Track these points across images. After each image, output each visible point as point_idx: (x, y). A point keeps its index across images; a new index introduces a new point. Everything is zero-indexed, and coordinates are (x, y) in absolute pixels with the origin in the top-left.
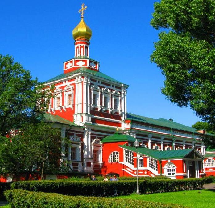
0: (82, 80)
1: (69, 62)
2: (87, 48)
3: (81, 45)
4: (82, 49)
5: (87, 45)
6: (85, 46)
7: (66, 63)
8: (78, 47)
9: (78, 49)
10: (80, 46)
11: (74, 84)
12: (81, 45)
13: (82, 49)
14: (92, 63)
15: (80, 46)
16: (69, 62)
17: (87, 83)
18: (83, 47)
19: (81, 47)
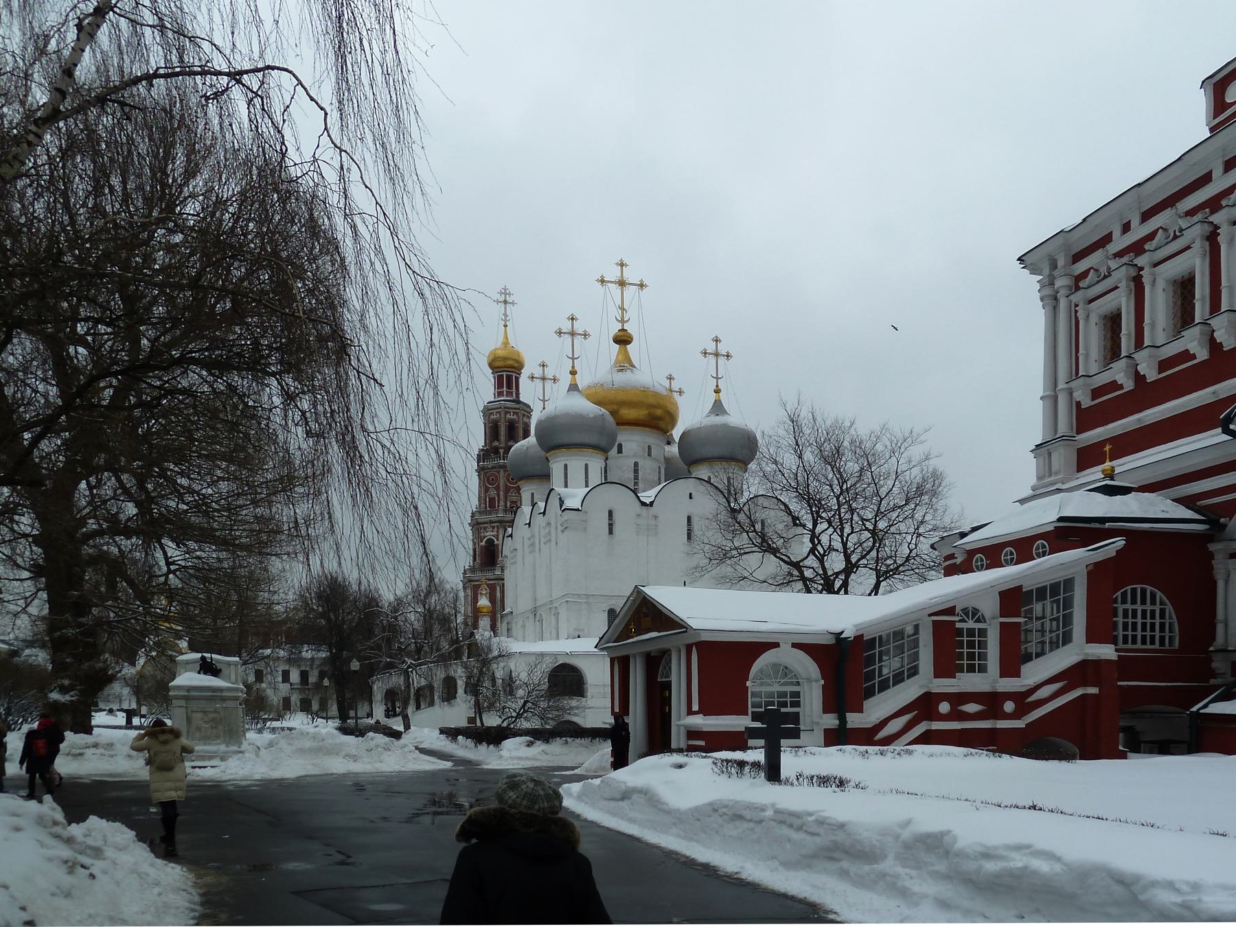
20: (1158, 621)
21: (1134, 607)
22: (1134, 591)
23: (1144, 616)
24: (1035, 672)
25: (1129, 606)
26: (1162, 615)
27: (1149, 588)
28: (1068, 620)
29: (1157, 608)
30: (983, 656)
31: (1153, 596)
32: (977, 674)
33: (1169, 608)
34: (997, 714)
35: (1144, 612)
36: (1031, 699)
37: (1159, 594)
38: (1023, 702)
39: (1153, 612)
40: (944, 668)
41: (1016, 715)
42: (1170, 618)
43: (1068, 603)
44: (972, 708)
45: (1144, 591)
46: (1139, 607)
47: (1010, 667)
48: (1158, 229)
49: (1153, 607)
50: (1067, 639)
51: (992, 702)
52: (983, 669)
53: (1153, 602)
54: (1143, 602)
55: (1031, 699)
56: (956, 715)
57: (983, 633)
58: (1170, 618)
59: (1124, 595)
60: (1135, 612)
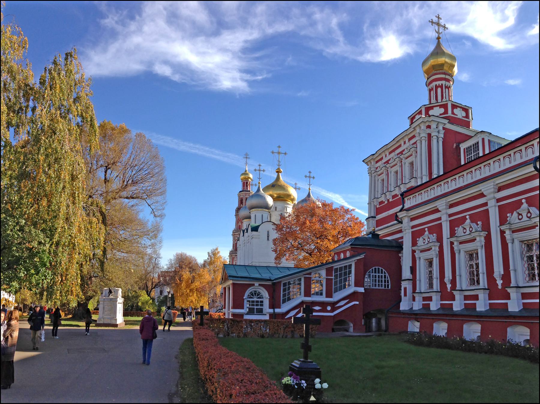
0: (428, 131)
1: (416, 115)
2: (448, 88)
3: (438, 85)
4: (439, 90)
5: (447, 83)
6: (445, 85)
7: (412, 118)
8: (432, 89)
9: (432, 92)
10: (436, 85)
11: (415, 143)
12: (438, 85)
13: (439, 90)
14: (459, 109)
15: (436, 85)
16: (416, 115)
17: (438, 138)
18: (441, 87)
19: (437, 87)
20: (383, 279)
21: (375, 274)
22: (375, 269)
23: (379, 278)
25: (374, 274)
26: (385, 277)
27: (380, 268)
29: (383, 275)
31: (382, 270)
33: (387, 274)
35: (379, 276)
37: (384, 270)
39: (382, 276)
42: (387, 278)
43: (350, 272)
45: (379, 269)
46: (377, 274)
49: (382, 274)
53: (382, 273)
54: (379, 273)
58: (387, 278)
59: (372, 270)
60: (376, 276)
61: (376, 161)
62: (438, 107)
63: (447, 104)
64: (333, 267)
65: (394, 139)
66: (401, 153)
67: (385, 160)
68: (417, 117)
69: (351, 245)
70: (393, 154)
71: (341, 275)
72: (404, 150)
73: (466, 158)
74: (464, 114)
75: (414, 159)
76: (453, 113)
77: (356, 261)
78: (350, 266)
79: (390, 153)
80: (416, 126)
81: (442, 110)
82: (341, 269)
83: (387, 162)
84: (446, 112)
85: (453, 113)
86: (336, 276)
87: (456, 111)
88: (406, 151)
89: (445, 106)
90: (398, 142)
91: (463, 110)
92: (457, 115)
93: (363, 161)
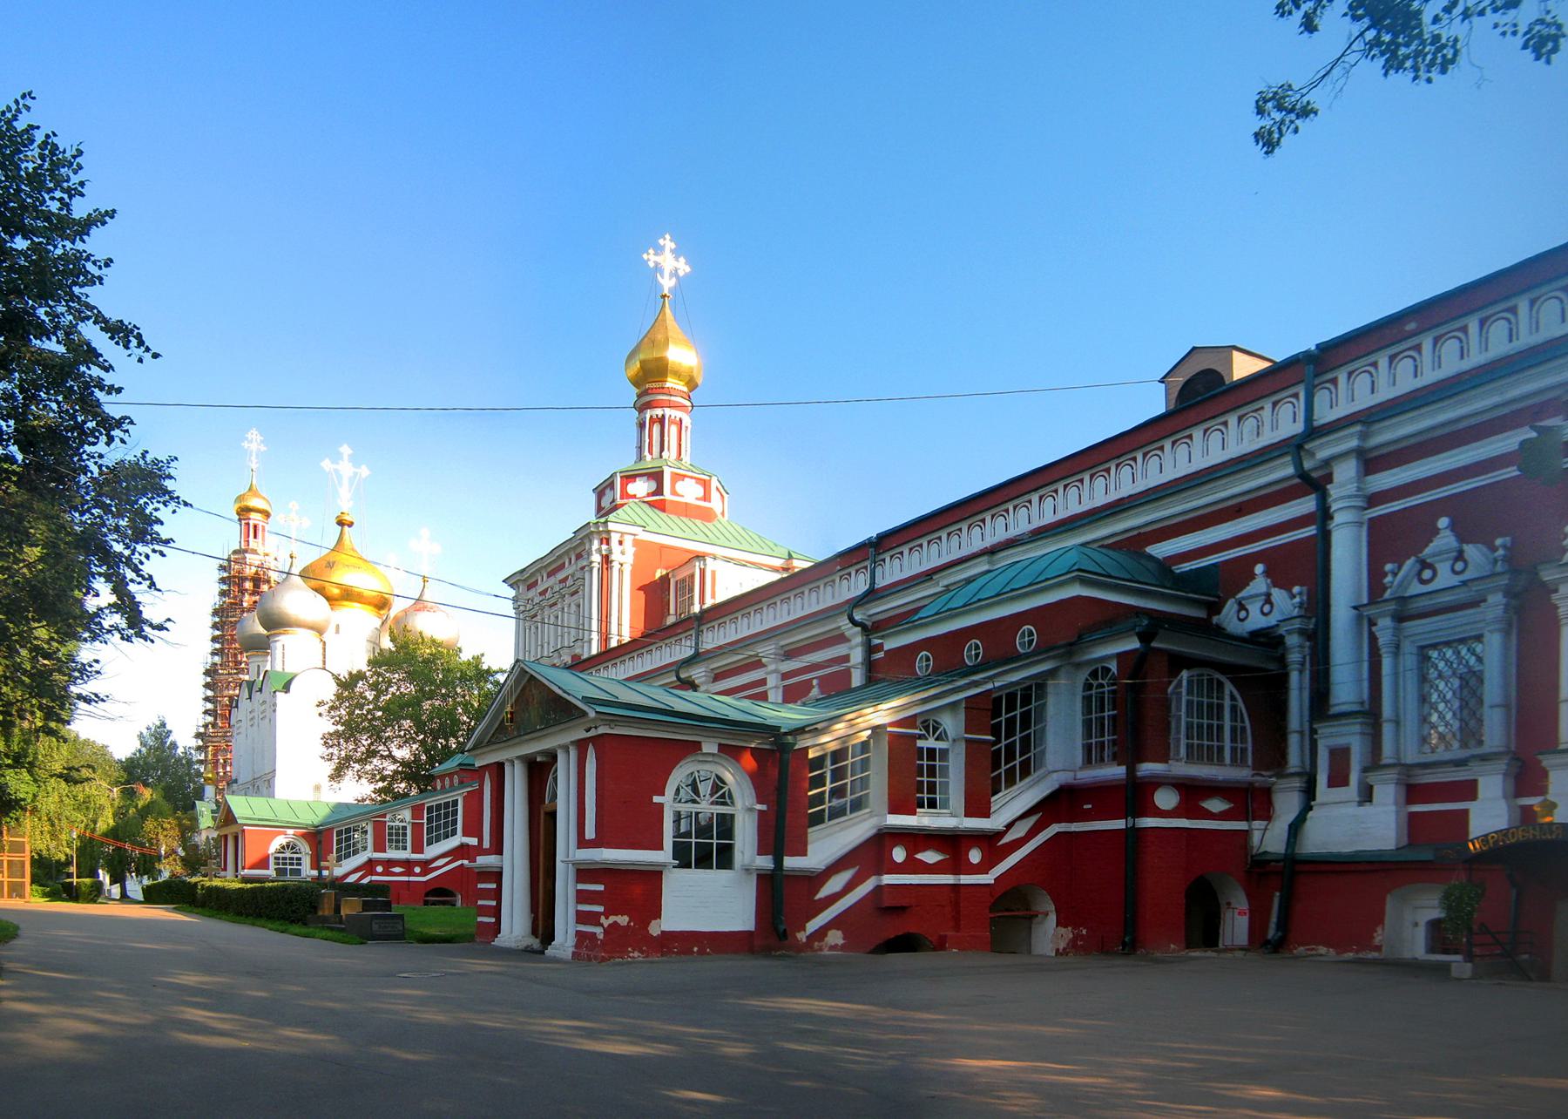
11: (583, 568)
16: (605, 488)
24: (431, 851)
28: (455, 822)
30: (404, 841)
32: (401, 851)
34: (409, 872)
36: (434, 865)
38: (426, 866)
40: (379, 847)
41: (423, 874)
43: (455, 813)
44: (398, 870)
47: (418, 848)
48: (547, 589)
50: (454, 833)
51: (408, 865)
52: (405, 848)
55: (434, 865)
56: (386, 873)
57: (404, 828)
61: (529, 583)
62: (645, 478)
63: (663, 472)
64: (424, 804)
65: (551, 552)
66: (565, 579)
67: (540, 588)
68: (608, 491)
69: (460, 764)
70: (552, 580)
71: (438, 817)
72: (566, 578)
73: (679, 600)
74: (700, 491)
75: (581, 600)
76: (674, 493)
77: (465, 794)
78: (455, 803)
79: (549, 575)
80: (585, 536)
81: (653, 486)
82: (439, 807)
83: (543, 593)
84: (659, 491)
85: (674, 493)
86: (430, 820)
87: (679, 486)
88: (570, 582)
89: (657, 476)
90: (559, 557)
91: (697, 483)
92: (682, 496)
93: (504, 581)
